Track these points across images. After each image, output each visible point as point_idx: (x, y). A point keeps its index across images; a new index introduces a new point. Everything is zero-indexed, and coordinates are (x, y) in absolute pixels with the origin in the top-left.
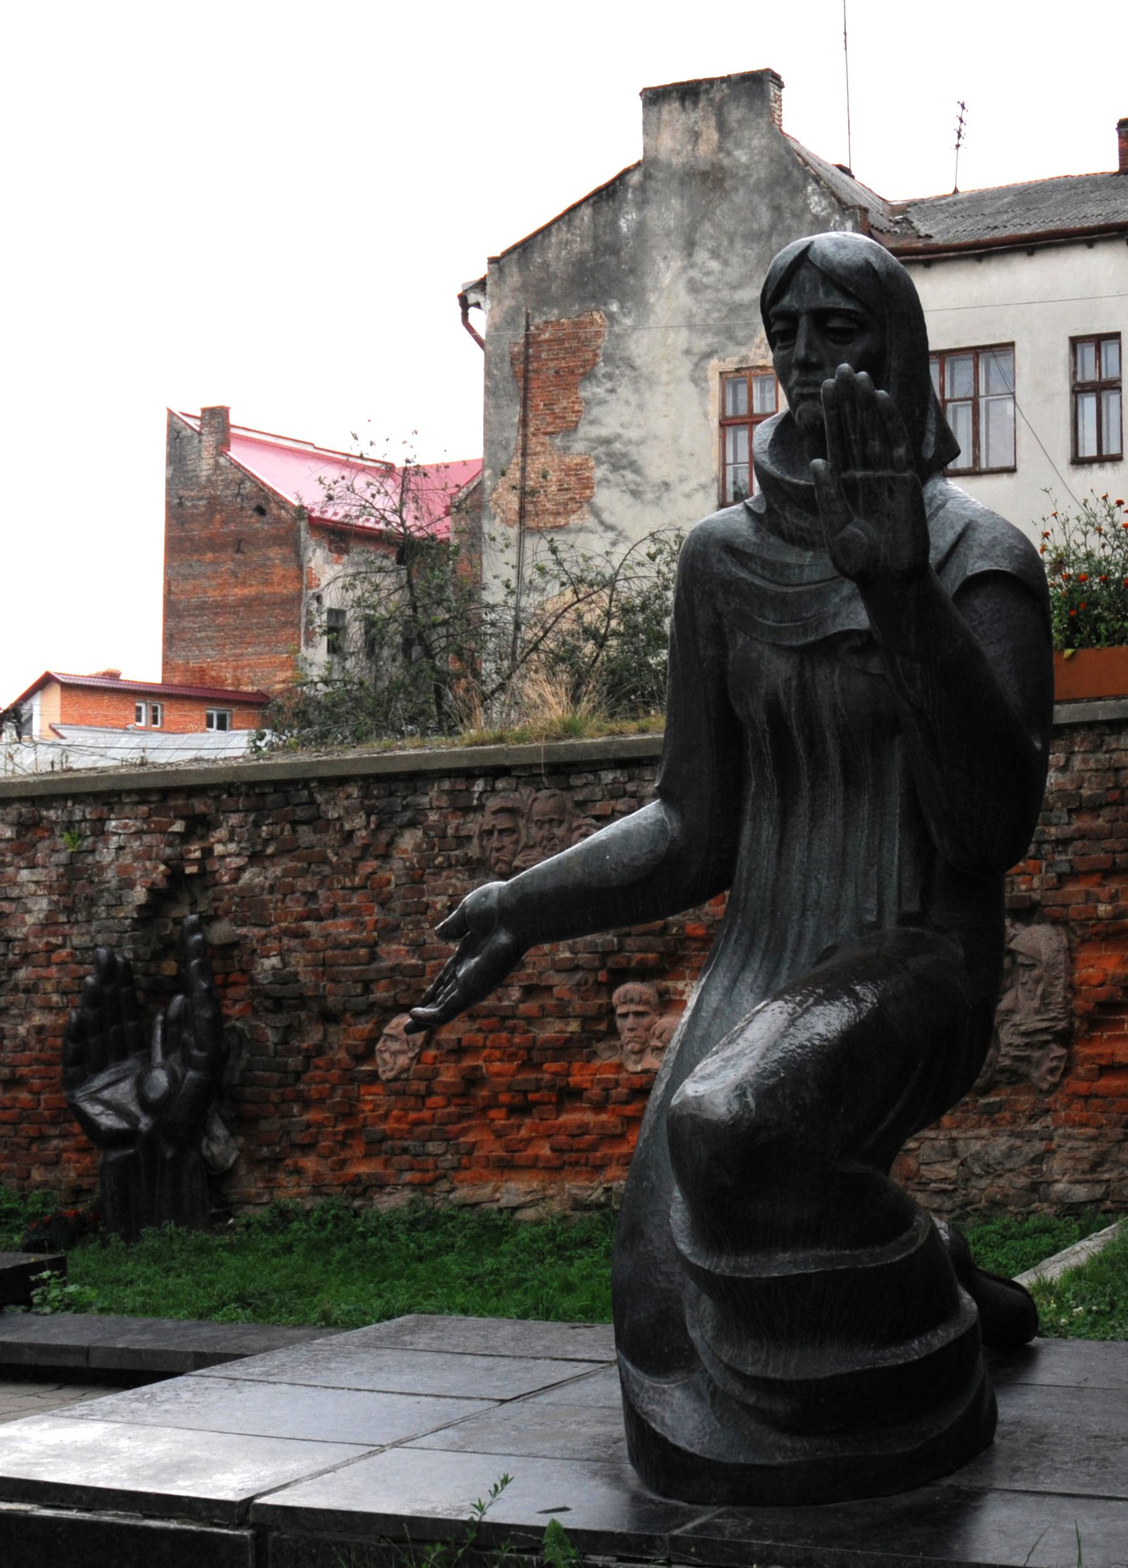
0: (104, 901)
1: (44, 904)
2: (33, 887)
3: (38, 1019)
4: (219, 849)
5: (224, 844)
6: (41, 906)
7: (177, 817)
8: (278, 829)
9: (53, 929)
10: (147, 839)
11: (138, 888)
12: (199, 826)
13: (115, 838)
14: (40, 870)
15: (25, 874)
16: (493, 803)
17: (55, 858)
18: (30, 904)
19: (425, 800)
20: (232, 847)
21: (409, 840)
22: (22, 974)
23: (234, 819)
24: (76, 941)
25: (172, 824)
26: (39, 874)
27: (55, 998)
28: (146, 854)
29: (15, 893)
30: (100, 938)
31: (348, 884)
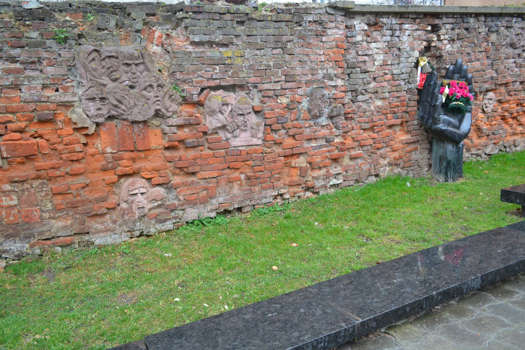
0: (404, 56)
1: (382, 57)
2: (377, 50)
3: (379, 103)
4: (442, 37)
5: (444, 35)
6: (380, 58)
7: (429, 25)
8: (460, 30)
9: (384, 67)
10: (419, 32)
11: (416, 51)
12: (435, 29)
13: (408, 31)
14: (379, 43)
15: (373, 45)
16: (517, 25)
17: (384, 38)
18: (376, 56)
19: (499, 23)
20: (447, 37)
21: (493, 37)
22: (373, 85)
23: (448, 26)
24: (395, 72)
25: (427, 27)
26: (379, 45)
27: (387, 95)
28: (419, 38)
29: (370, 53)
30: (403, 70)
31: (480, 50)
